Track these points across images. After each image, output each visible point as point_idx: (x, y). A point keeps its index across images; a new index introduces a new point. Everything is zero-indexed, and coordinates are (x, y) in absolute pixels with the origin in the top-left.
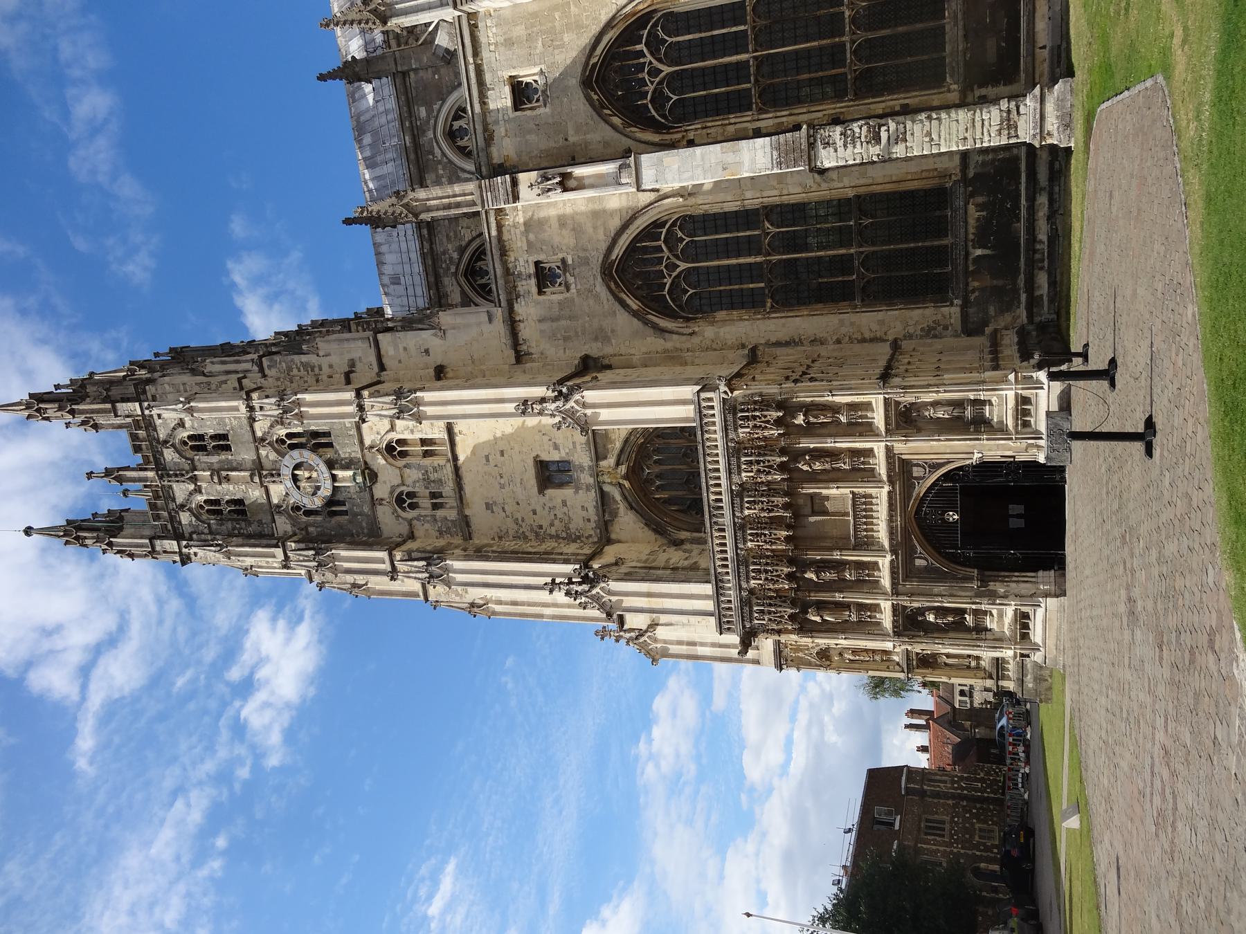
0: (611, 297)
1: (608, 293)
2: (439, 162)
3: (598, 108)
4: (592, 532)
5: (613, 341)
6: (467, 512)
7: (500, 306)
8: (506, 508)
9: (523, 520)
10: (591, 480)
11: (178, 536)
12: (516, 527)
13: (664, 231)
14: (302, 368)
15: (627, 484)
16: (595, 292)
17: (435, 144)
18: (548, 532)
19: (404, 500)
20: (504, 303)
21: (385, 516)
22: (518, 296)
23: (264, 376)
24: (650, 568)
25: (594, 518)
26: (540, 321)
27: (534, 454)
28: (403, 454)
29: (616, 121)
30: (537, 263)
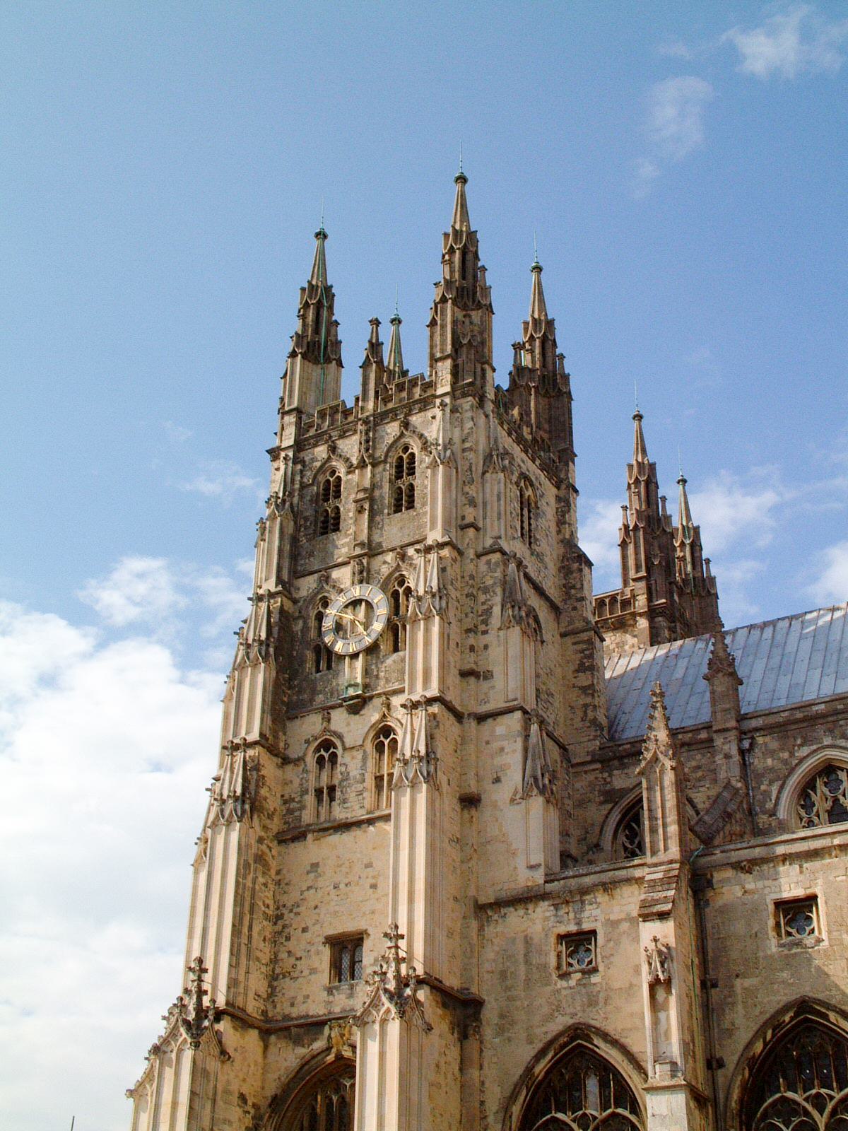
0: (549, 1037)
1: (554, 1034)
2: (792, 754)
3: (774, 1022)
4: (278, 1009)
5: (497, 1040)
6: (310, 836)
7: (546, 882)
8: (312, 891)
9: (298, 914)
10: (337, 1009)
11: (299, 446)
12: (289, 904)
13: (626, 1113)
14: (485, 607)
15: (331, 1058)
16: (556, 1014)
17: (814, 747)
18: (282, 949)
19: (327, 750)
20: (549, 887)
21: (311, 725)
22: (556, 907)
23: (479, 556)
24: (214, 1101)
25: (295, 1012)
26: (526, 937)
27: (370, 931)
28: (380, 748)
29: (759, 1047)
30: (594, 932)
